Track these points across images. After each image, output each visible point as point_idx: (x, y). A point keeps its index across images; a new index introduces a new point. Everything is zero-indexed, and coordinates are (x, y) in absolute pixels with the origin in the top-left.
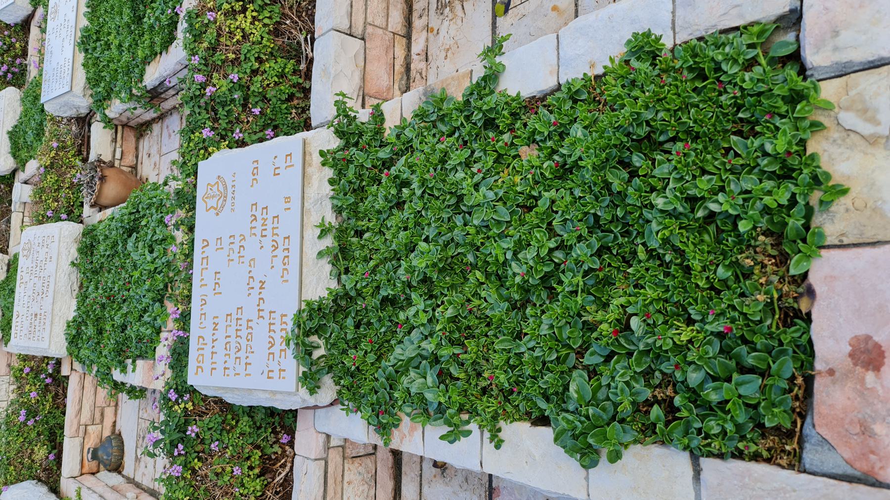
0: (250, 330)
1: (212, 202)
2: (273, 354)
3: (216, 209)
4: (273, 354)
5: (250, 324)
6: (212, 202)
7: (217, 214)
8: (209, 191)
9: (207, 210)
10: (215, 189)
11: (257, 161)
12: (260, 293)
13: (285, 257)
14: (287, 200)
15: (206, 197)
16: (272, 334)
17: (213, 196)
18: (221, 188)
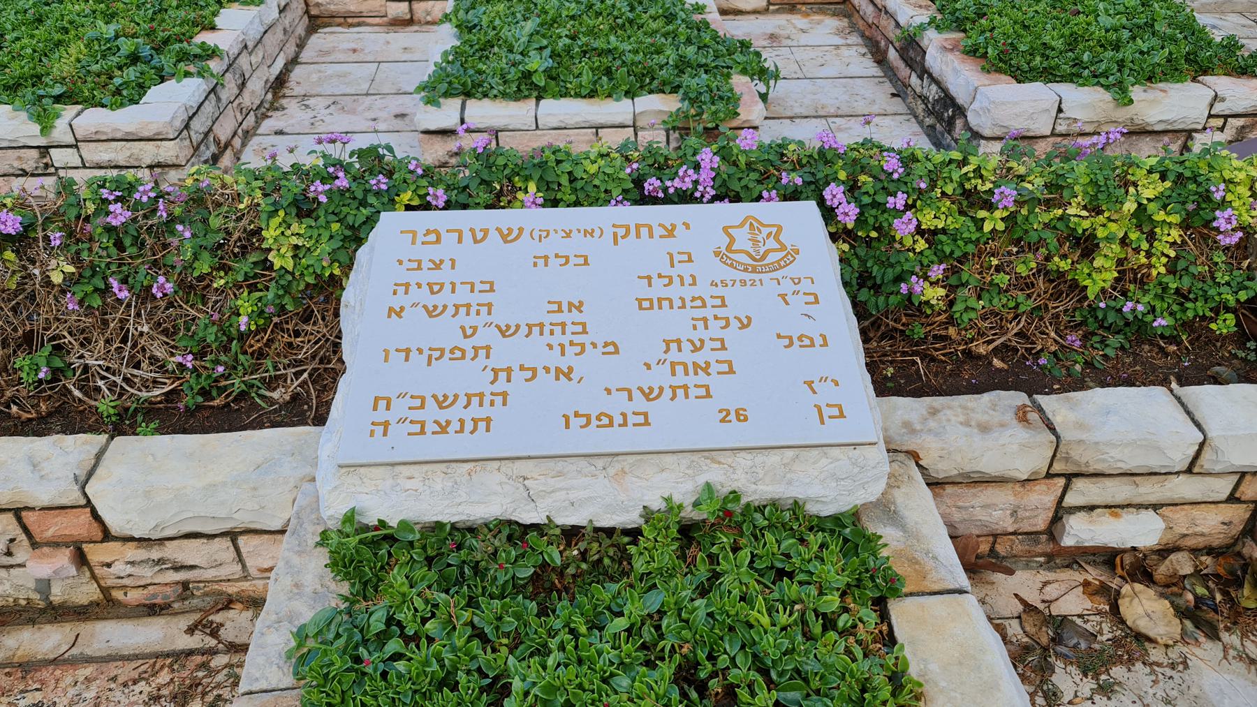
0: (470, 354)
1: (743, 239)
2: (422, 407)
3: (729, 248)
4: (422, 407)
5: (482, 353)
6: (743, 239)
7: (717, 254)
8: (765, 231)
9: (725, 229)
10: (772, 244)
11: (825, 344)
12: (547, 370)
13: (611, 418)
14: (741, 416)
15: (753, 224)
16: (462, 401)
17: (755, 241)
18: (772, 258)
